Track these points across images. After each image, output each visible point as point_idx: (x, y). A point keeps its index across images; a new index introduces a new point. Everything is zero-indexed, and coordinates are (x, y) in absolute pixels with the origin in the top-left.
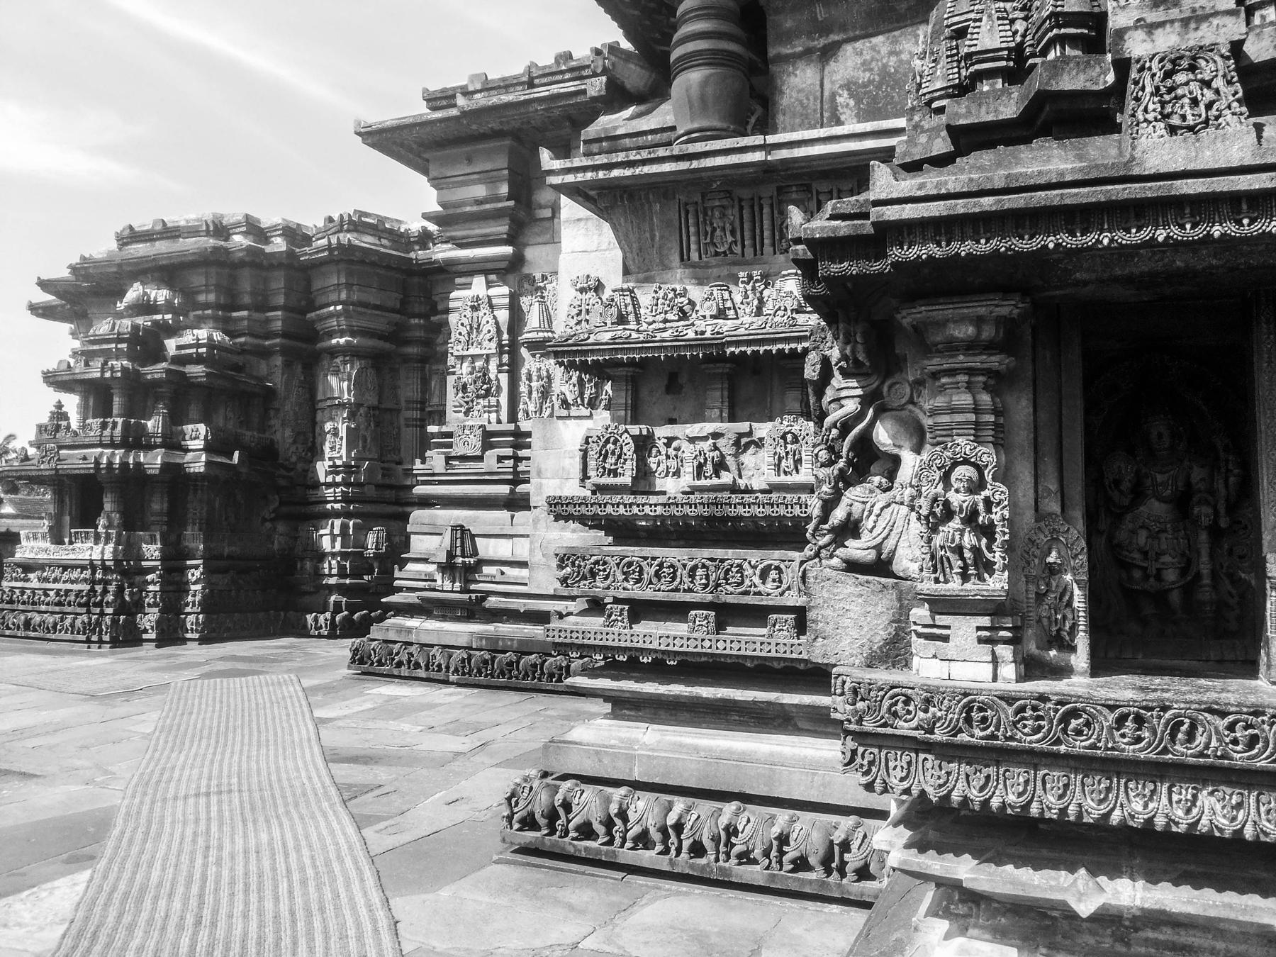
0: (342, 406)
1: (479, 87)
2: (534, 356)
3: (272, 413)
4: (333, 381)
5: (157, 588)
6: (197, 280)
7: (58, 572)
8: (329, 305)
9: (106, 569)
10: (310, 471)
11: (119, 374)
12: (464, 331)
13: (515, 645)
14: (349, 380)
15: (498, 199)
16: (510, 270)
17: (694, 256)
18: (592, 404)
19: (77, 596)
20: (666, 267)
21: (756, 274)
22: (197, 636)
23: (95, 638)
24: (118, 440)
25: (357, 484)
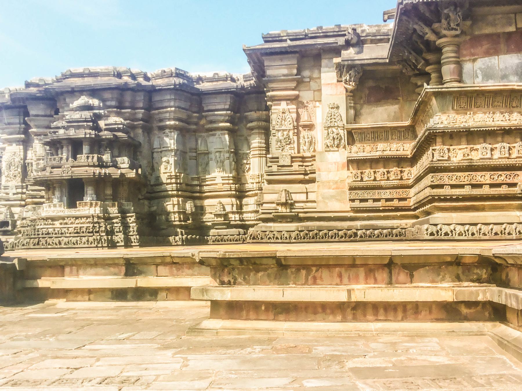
0: (171, 150)
1: (285, 35)
2: (305, 130)
3: (138, 153)
4: (167, 140)
5: (120, 225)
6: (107, 95)
7: (73, 220)
8: (166, 107)
9: (99, 217)
10: (158, 178)
11: (93, 136)
12: (279, 121)
13: (316, 228)
14: (174, 139)
15: (292, 75)
16: (295, 100)
17: (455, 108)
18: (338, 146)
19: (87, 229)
20: (448, 110)
21: (472, 113)
22: (138, 244)
23: (100, 245)
24: (97, 163)
25: (180, 184)
